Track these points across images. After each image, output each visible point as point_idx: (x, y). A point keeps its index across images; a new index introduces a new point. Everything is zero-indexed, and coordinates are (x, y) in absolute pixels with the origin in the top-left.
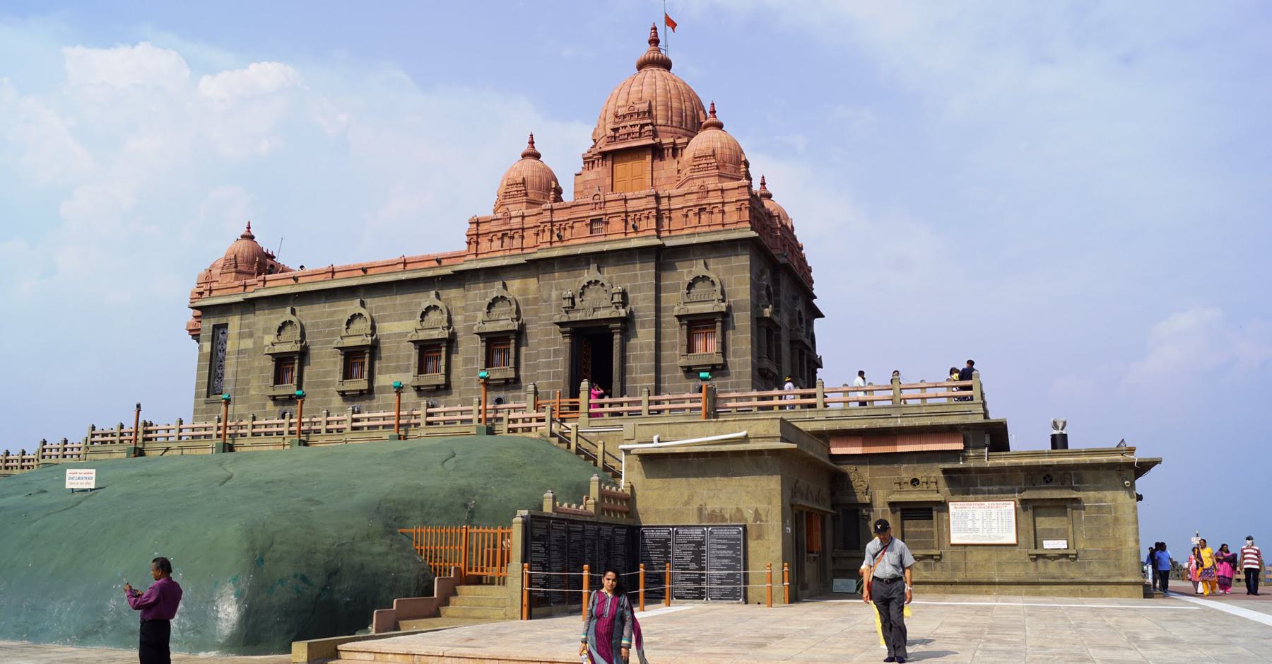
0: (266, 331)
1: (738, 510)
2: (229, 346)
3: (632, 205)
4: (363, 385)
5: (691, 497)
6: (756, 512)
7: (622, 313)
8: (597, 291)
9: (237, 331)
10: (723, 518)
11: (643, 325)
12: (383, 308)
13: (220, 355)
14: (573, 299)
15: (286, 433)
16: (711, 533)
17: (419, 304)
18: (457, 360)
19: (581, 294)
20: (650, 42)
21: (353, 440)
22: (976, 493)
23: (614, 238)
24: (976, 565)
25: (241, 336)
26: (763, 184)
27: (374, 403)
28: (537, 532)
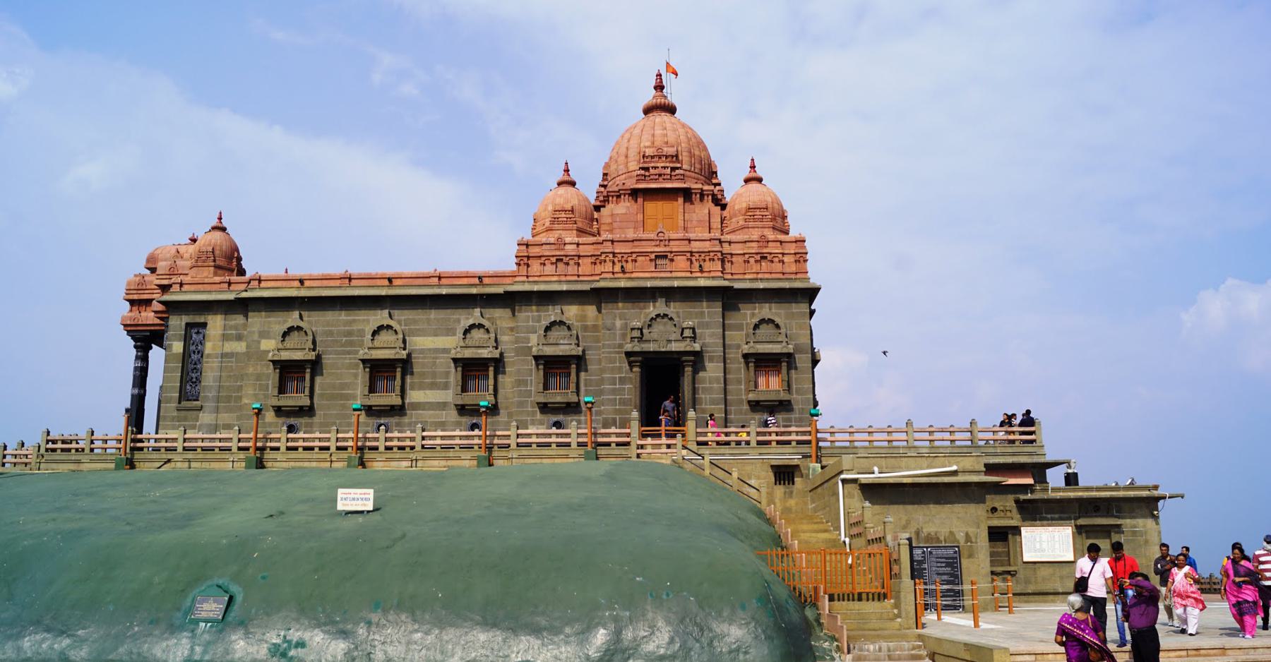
0: (264, 335)
1: (951, 533)
2: (209, 348)
3: (696, 246)
4: (394, 399)
5: (908, 522)
6: (967, 534)
8: (665, 324)
10: (938, 540)
11: (711, 360)
12: (415, 322)
13: (195, 357)
14: (641, 330)
15: (333, 449)
17: (459, 321)
18: (506, 381)
19: (649, 326)
20: (656, 88)
21: (424, 459)
22: (1042, 519)
23: (679, 275)
24: (1044, 579)
25: (225, 338)
27: (406, 420)
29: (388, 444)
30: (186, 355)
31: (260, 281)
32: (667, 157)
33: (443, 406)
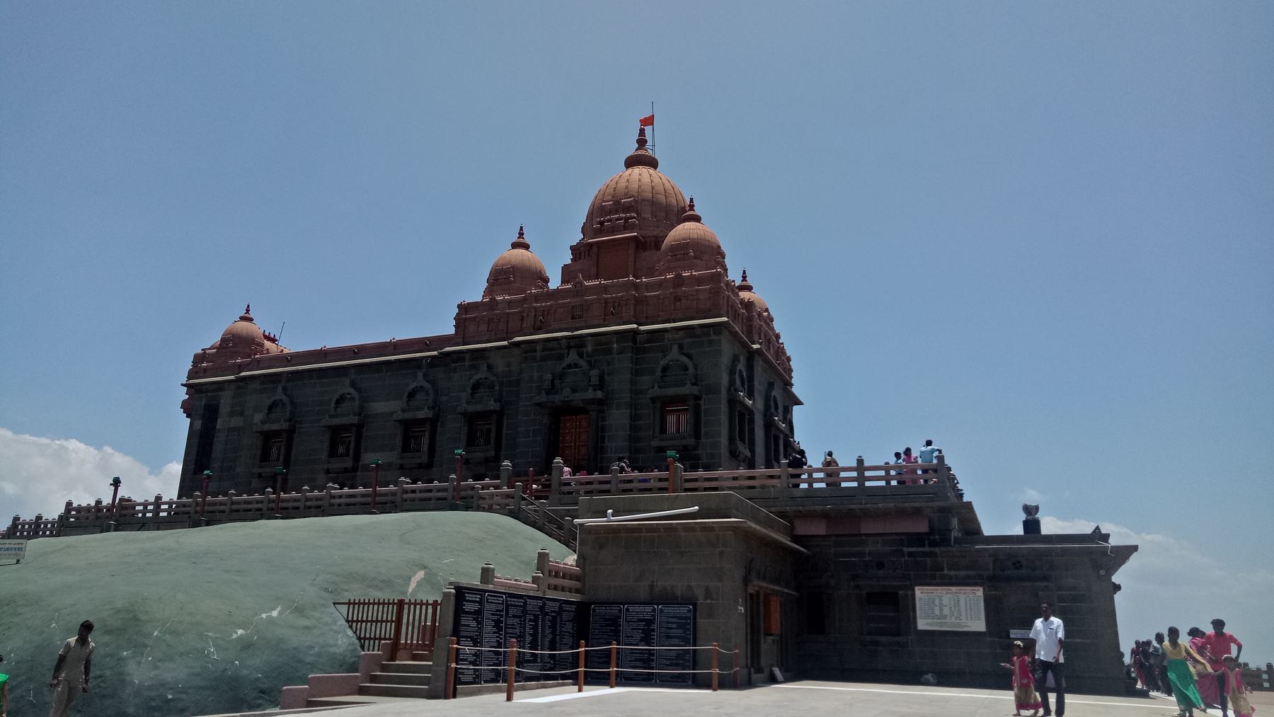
2: (220, 424)
4: (349, 463)
6: (707, 589)
7: (599, 394)
16: (661, 611)
25: (232, 414)
26: (744, 278)
28: (469, 607)
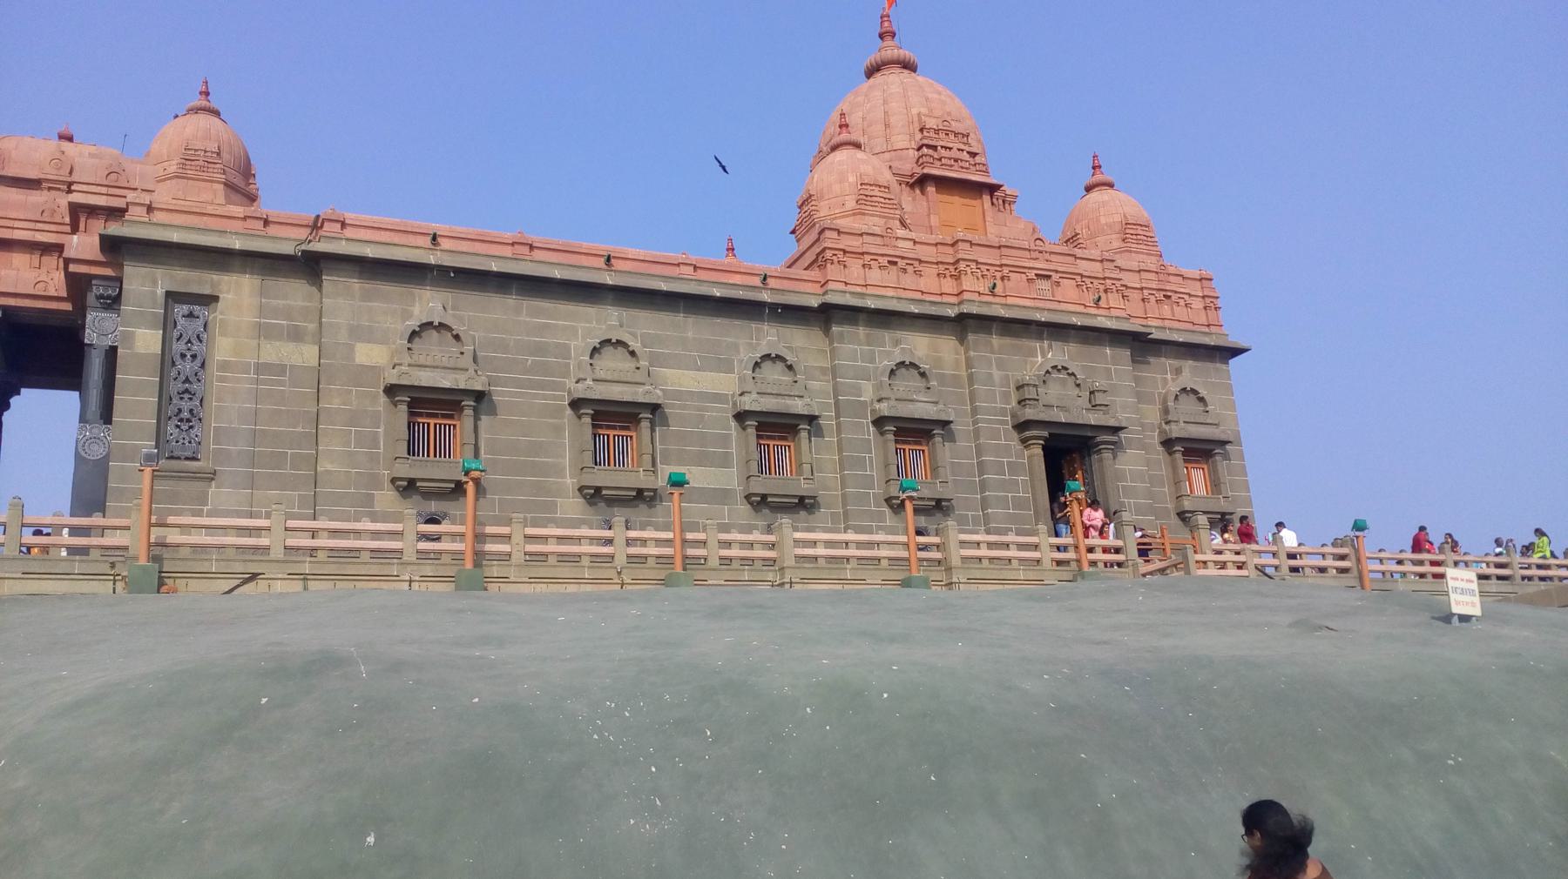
0: (361, 333)
2: (222, 349)
9: (249, 318)
15: (621, 560)
25: (263, 332)
29: (725, 553)
30: (166, 361)
31: (344, 225)
32: (956, 134)
33: (722, 496)
